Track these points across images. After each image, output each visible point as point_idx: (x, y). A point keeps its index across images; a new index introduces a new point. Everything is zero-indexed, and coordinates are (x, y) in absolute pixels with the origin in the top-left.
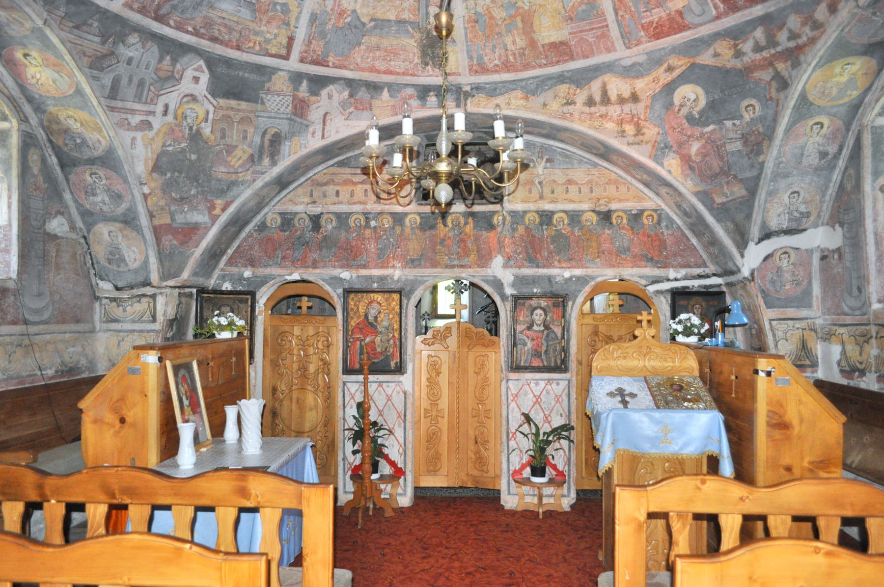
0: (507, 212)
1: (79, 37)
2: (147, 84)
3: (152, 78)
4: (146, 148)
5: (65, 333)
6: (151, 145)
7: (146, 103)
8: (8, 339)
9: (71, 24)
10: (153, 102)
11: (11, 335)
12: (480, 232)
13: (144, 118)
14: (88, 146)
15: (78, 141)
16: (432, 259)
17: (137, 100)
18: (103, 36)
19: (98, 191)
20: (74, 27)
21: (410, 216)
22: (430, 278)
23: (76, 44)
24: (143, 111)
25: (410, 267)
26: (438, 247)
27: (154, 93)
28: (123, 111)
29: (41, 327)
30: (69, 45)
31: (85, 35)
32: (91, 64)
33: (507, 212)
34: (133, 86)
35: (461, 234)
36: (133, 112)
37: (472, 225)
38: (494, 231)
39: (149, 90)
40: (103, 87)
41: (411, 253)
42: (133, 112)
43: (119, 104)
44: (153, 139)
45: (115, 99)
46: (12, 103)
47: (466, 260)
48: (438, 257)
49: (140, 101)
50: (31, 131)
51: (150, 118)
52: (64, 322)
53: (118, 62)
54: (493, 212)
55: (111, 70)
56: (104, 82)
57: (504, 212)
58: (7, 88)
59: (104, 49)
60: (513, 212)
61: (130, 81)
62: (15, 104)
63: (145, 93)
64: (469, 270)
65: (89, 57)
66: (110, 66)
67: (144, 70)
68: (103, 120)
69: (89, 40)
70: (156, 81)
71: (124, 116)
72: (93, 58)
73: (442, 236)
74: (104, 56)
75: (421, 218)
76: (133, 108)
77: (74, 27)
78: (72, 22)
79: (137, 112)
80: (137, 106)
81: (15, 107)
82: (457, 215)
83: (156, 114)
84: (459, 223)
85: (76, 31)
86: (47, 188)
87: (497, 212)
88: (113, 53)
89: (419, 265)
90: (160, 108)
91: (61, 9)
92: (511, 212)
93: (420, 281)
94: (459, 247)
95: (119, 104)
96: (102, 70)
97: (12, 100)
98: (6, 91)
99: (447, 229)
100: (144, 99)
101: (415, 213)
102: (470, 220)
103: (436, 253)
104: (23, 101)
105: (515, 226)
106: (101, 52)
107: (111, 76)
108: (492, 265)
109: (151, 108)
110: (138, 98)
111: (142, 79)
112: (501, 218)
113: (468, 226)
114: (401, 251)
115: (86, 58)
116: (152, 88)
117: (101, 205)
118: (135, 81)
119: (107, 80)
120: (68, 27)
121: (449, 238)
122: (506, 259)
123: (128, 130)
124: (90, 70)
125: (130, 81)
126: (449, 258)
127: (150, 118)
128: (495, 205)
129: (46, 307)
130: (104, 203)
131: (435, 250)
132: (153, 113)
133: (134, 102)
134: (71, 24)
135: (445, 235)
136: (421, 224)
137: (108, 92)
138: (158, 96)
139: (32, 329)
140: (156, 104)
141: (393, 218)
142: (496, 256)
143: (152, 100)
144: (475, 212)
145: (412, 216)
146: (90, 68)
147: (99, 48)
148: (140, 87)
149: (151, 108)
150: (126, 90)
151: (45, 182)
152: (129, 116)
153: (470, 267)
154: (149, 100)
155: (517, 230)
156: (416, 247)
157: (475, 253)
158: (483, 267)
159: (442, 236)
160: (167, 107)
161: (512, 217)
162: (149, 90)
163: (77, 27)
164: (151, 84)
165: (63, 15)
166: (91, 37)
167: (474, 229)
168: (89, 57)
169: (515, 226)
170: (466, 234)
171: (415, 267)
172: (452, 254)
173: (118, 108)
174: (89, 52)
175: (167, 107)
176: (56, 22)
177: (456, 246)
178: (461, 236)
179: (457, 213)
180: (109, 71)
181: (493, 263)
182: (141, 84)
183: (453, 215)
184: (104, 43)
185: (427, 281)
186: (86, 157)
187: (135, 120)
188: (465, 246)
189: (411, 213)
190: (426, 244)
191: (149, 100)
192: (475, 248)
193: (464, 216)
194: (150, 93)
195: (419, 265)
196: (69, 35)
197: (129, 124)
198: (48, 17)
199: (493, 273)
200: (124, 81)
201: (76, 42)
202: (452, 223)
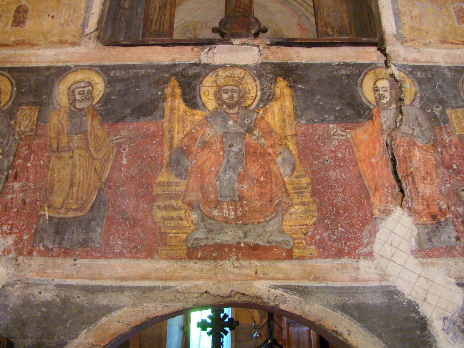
0: (402, 68)
12: (320, 129)
16: (135, 223)
21: (72, 78)
22: (125, 298)
25: (47, 252)
26: (163, 177)
33: (402, 68)
35: (250, 130)
37: (288, 103)
38: (368, 126)
41: (58, 200)
47: (273, 226)
48: (159, 214)
54: (355, 65)
57: (394, 70)
60: (422, 68)
64: (284, 265)
73: (177, 138)
75: (110, 82)
82: (238, 72)
84: (242, 97)
87: (371, 66)
89: (84, 244)
92: (414, 67)
93: (81, 309)
94: (241, 178)
99: (199, 115)
101: (91, 68)
102: (282, 84)
103: (154, 199)
105: (437, 111)
108: (376, 247)
112: (384, 84)
113: (275, 106)
114: (23, 190)
121: (205, 144)
122: (426, 220)
126: (204, 218)
128: (361, 48)
131: (149, 186)
135: (191, 136)
136: (106, 100)
141: (19, 84)
142: (387, 212)
144: (297, 66)
145: (79, 76)
153: (290, 256)
155: (446, 121)
156: (79, 175)
157: (307, 198)
158: (340, 254)
159: (177, 138)
161: (420, 82)
167: (297, 117)
169: (437, 111)
170: (269, 132)
171: (66, 254)
172: (218, 204)
177: (230, 174)
178: (250, 139)
179: (234, 66)
181: (381, 236)
183: (221, 73)
185: (109, 310)
188: (268, 174)
189: (78, 68)
190: (117, 167)
192: (305, 181)
193: (260, 76)
195: (84, 244)
199: (384, 276)
202: (218, 96)
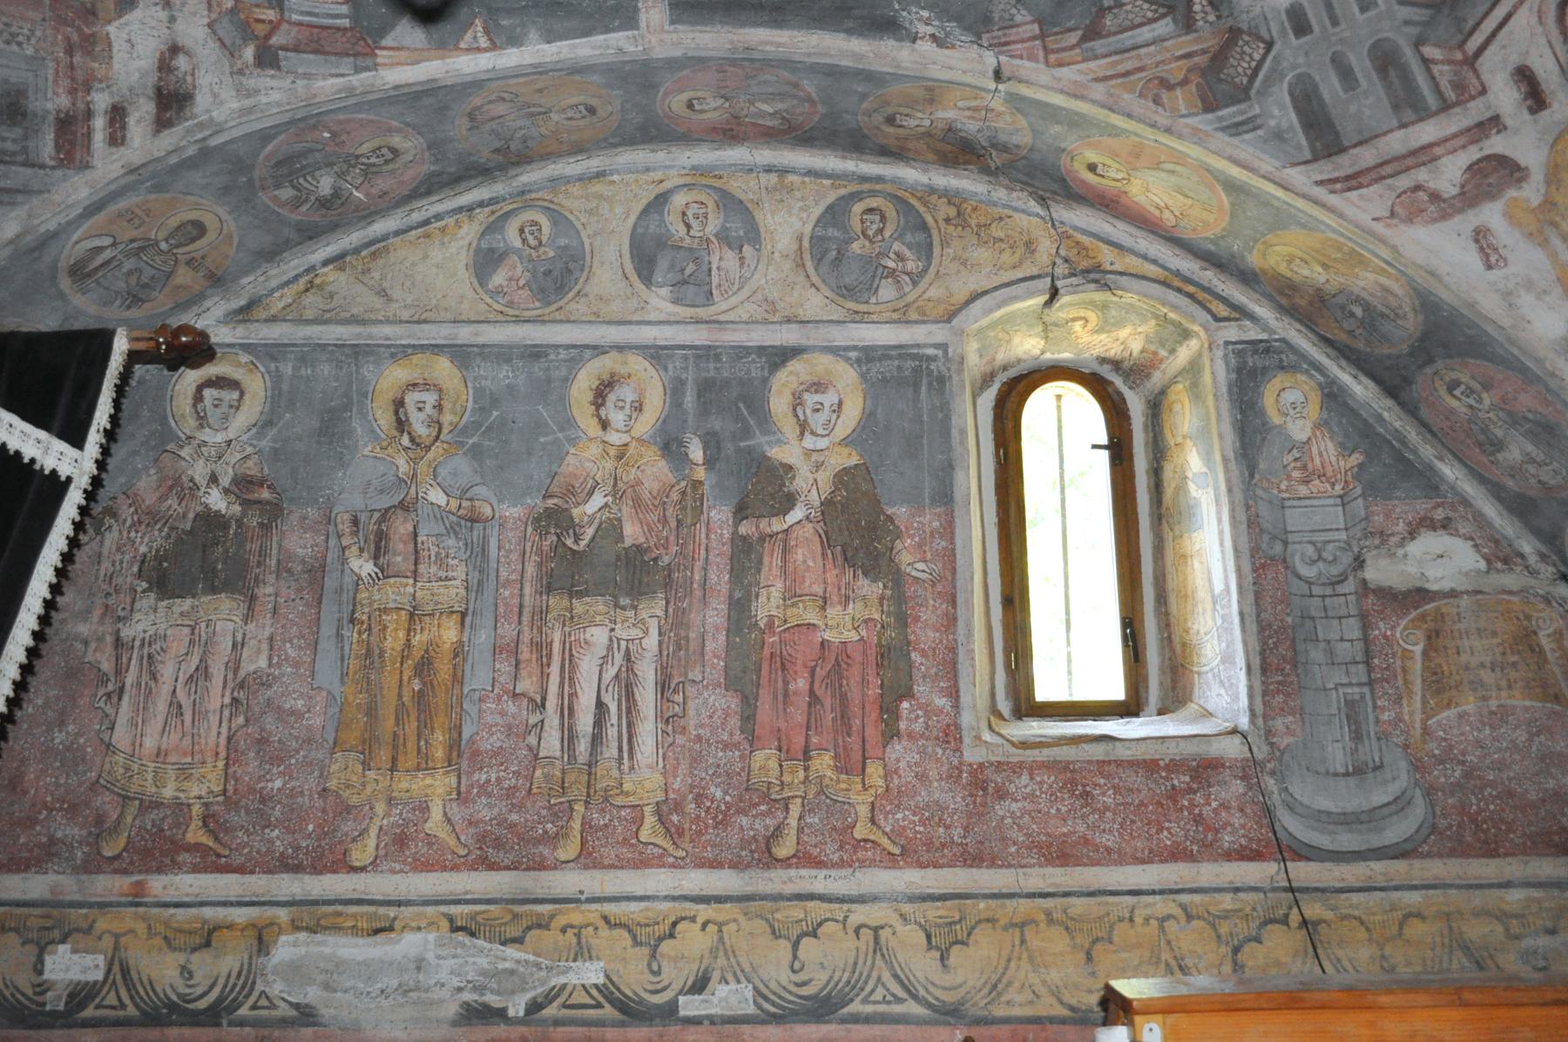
1: (1116, 53)
2: (1408, 53)
3: (1407, 23)
4: (1544, 243)
5: (1507, 885)
6: (1554, 225)
7: (1446, 107)
8: (1227, 902)
9: (1073, 38)
10: (1467, 90)
11: (1237, 890)
13: (1474, 153)
14: (1383, 315)
15: (1358, 311)
17: (1409, 115)
18: (1171, 9)
19: (1499, 433)
20: (1085, 38)
23: (1127, 74)
24: (1455, 136)
27: (1450, 62)
28: (1387, 170)
29: (1378, 867)
30: (1099, 91)
31: (1127, 38)
32: (1203, 99)
34: (1363, 82)
36: (1424, 155)
39: (1426, 62)
40: (1278, 136)
42: (1424, 155)
43: (1366, 156)
44: (1548, 204)
45: (1343, 150)
46: (1179, 290)
49: (1423, 114)
50: (1264, 336)
51: (1496, 144)
52: (1490, 850)
53: (1269, 45)
55: (1267, 78)
56: (1272, 123)
58: (1154, 262)
59: (1206, 38)
61: (1347, 75)
62: (1191, 289)
63: (1421, 79)
65: (1184, 82)
66: (1256, 71)
67: (1360, 17)
68: (1334, 225)
69: (1148, 45)
70: (1425, 24)
71: (1404, 182)
72: (1196, 79)
74: (1219, 57)
76: (1415, 144)
77: (1085, 38)
78: (1070, 30)
79: (1437, 151)
80: (1427, 132)
81: (1191, 296)
83: (1508, 122)
85: (1098, 45)
86: (1360, 466)
88: (1235, 33)
90: (1505, 97)
91: (1018, 18)
95: (1366, 156)
96: (1241, 94)
97: (1177, 283)
98: (1153, 268)
100: (1432, 101)
104: (1210, 276)
106: (1204, 52)
107: (1282, 93)
109: (1476, 111)
110: (1410, 106)
111: (1375, 46)
115: (1178, 92)
116: (1429, 51)
117: (1532, 469)
118: (1360, 63)
119: (1280, 111)
120: (1072, 48)
123: (1444, 216)
124: (1210, 116)
125: (1347, 75)
127: (1496, 144)
129: (1400, 804)
130: (1533, 461)
132: (1494, 123)
133: (1403, 126)
134: (1073, 38)
137: (1304, 142)
138: (1471, 61)
139: (1304, 872)
140: (1483, 91)
143: (1459, 86)
146: (1208, 108)
147: (1186, 43)
148: (1392, 73)
149: (1476, 111)
150: (1353, 108)
151: (1345, 449)
152: (1422, 175)
154: (1451, 95)
160: (1525, 77)
162: (1426, 62)
163: (1092, 33)
164: (1418, 43)
165: (1036, 28)
166: (1145, 33)
168: (1184, 82)
173: (1369, 170)
174: (1176, 71)
175: (1525, 77)
176: (1032, 58)
180: (1268, 81)
182: (1385, 60)
184: (1188, 24)
186: (1405, 349)
187: (1449, 174)
191: (1451, 95)
194: (1436, 69)
196: (1092, 65)
197: (1435, 197)
198: (1003, 59)
200: (1330, 87)
201: (1121, 68)
